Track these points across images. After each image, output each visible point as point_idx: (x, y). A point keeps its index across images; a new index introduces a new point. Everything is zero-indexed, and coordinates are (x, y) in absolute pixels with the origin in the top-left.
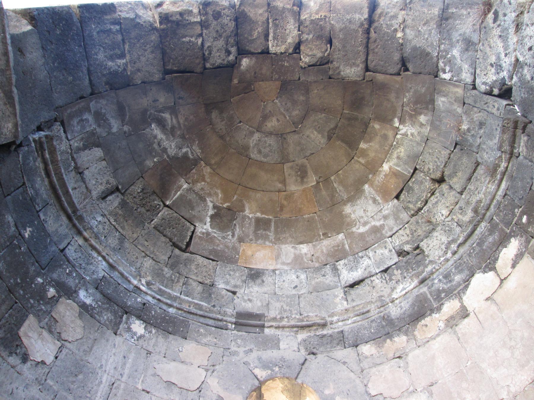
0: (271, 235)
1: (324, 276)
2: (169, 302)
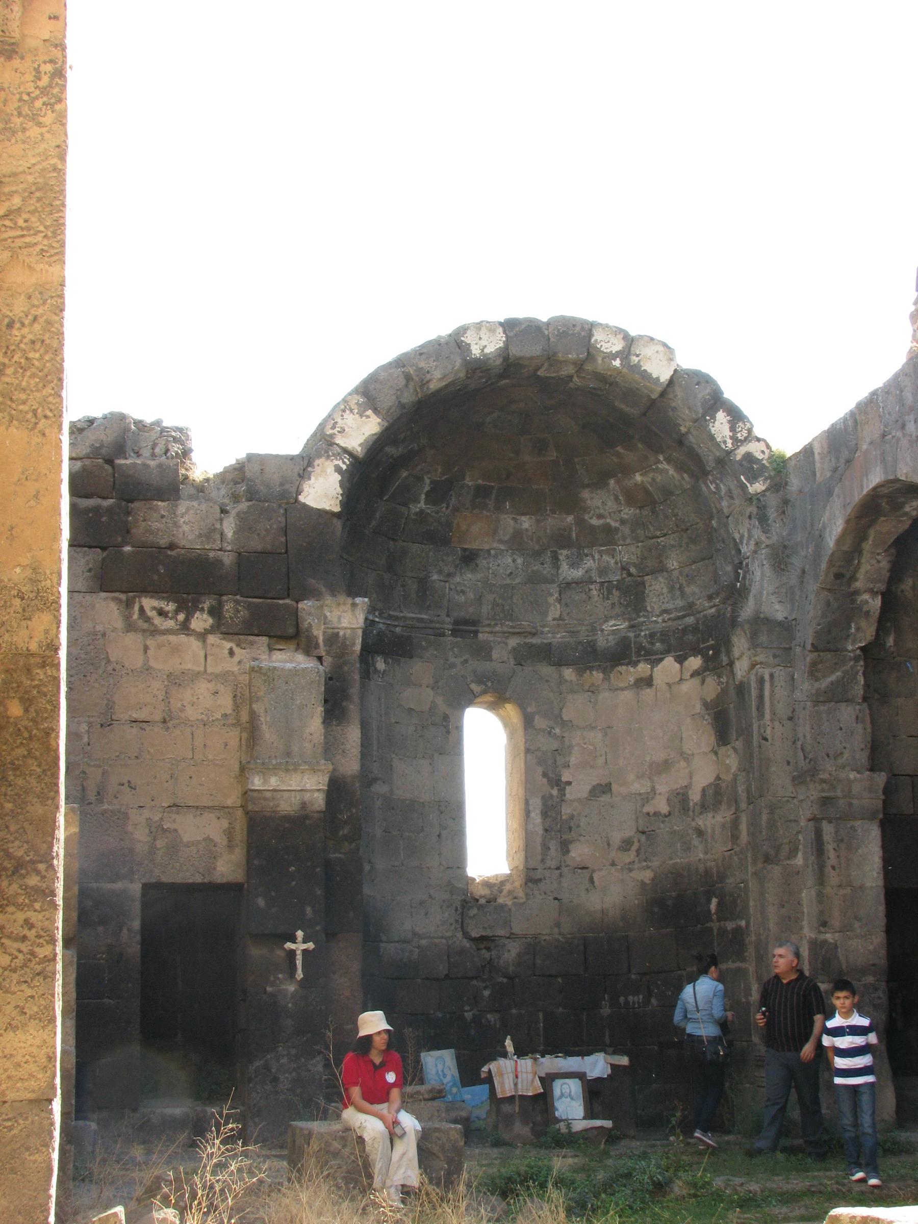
0: (491, 503)
1: (542, 564)
2: (396, 623)
